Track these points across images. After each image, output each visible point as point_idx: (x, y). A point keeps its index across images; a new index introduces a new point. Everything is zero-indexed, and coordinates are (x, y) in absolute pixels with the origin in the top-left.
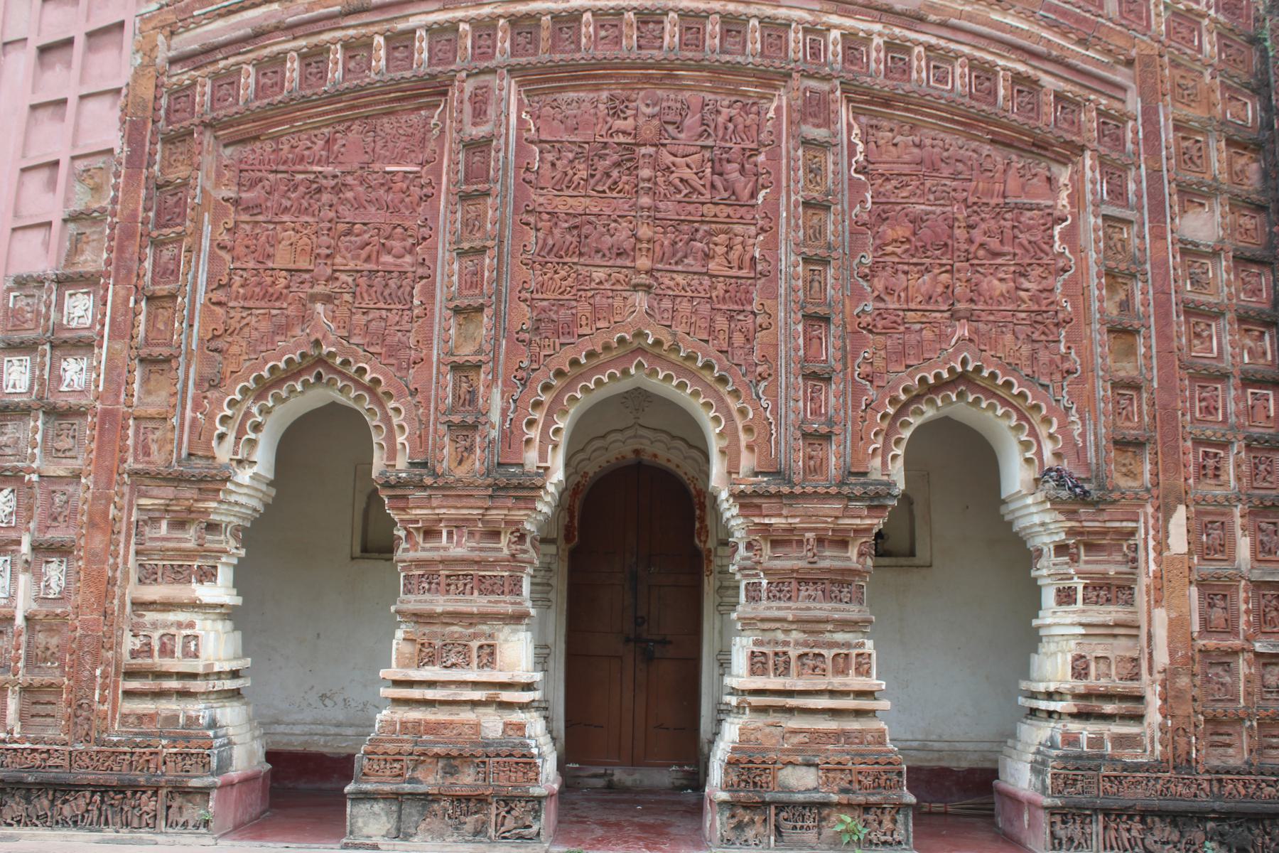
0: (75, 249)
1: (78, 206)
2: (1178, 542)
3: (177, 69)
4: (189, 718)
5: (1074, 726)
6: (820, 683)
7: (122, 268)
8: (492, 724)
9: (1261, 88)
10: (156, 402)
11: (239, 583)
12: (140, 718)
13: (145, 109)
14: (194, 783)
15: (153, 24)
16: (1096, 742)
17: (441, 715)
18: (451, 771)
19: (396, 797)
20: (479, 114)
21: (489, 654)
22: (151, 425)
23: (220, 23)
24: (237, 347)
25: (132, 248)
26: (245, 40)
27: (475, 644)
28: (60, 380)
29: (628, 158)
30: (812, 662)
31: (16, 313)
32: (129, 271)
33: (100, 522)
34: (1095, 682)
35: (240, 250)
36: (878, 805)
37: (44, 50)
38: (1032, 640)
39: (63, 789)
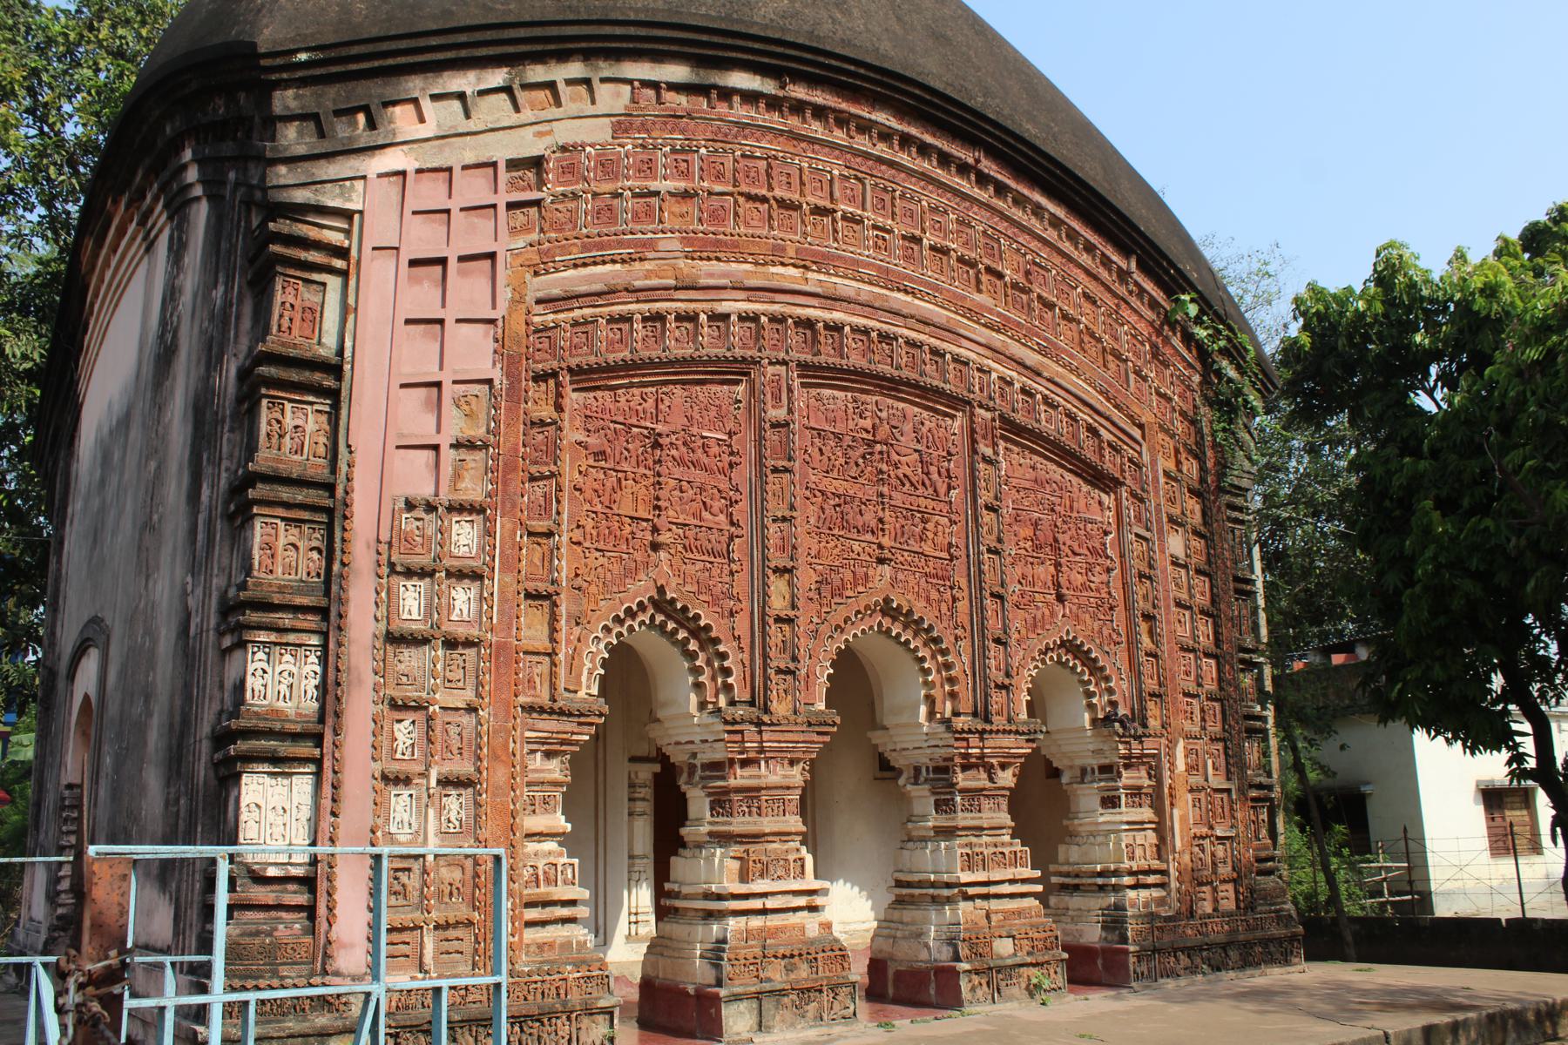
0: (457, 476)
3: (539, 309)
4: (578, 943)
5: (1132, 894)
6: (1009, 873)
9: (1199, 457)
12: (541, 947)
13: (519, 343)
14: (602, 1003)
15: (520, 261)
17: (774, 921)
18: (789, 969)
19: (758, 996)
22: (535, 658)
23: (571, 273)
26: (599, 294)
27: (791, 857)
28: (450, 608)
32: (514, 506)
35: (589, 494)
36: (1048, 962)
37: (414, 263)
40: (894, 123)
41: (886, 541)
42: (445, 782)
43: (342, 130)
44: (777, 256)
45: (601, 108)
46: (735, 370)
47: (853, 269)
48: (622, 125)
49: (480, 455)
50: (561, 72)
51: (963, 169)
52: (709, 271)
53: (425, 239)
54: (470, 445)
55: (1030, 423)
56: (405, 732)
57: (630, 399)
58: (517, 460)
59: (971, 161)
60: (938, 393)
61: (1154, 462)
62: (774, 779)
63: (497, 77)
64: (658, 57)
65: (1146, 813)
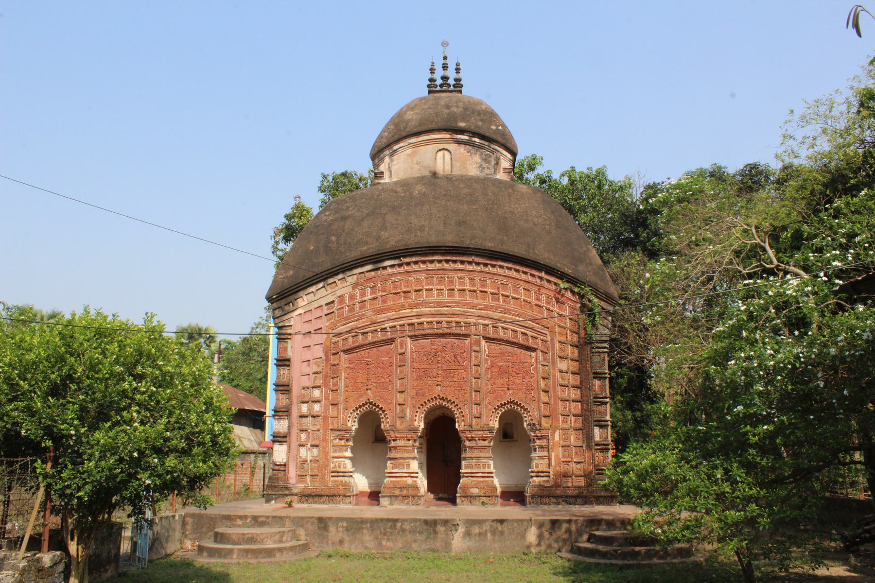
0: (315, 380)
2: (557, 438)
5: (535, 478)
7: (326, 384)
8: (410, 481)
10: (335, 413)
11: (352, 452)
16: (539, 482)
19: (390, 496)
20: (402, 346)
21: (408, 465)
25: (328, 380)
29: (435, 356)
30: (478, 466)
31: (304, 395)
33: (325, 440)
34: (540, 469)
38: (530, 460)
39: (320, 496)
40: (441, 258)
41: (439, 379)
42: (312, 446)
43: (287, 308)
44: (403, 307)
46: (392, 341)
47: (427, 304)
48: (355, 285)
49: (320, 375)
51: (470, 263)
54: (317, 373)
55: (496, 336)
56: (303, 436)
57: (361, 354)
58: (331, 373)
59: (471, 260)
60: (459, 335)
61: (552, 340)
63: (321, 285)
64: (362, 266)
65: (546, 453)
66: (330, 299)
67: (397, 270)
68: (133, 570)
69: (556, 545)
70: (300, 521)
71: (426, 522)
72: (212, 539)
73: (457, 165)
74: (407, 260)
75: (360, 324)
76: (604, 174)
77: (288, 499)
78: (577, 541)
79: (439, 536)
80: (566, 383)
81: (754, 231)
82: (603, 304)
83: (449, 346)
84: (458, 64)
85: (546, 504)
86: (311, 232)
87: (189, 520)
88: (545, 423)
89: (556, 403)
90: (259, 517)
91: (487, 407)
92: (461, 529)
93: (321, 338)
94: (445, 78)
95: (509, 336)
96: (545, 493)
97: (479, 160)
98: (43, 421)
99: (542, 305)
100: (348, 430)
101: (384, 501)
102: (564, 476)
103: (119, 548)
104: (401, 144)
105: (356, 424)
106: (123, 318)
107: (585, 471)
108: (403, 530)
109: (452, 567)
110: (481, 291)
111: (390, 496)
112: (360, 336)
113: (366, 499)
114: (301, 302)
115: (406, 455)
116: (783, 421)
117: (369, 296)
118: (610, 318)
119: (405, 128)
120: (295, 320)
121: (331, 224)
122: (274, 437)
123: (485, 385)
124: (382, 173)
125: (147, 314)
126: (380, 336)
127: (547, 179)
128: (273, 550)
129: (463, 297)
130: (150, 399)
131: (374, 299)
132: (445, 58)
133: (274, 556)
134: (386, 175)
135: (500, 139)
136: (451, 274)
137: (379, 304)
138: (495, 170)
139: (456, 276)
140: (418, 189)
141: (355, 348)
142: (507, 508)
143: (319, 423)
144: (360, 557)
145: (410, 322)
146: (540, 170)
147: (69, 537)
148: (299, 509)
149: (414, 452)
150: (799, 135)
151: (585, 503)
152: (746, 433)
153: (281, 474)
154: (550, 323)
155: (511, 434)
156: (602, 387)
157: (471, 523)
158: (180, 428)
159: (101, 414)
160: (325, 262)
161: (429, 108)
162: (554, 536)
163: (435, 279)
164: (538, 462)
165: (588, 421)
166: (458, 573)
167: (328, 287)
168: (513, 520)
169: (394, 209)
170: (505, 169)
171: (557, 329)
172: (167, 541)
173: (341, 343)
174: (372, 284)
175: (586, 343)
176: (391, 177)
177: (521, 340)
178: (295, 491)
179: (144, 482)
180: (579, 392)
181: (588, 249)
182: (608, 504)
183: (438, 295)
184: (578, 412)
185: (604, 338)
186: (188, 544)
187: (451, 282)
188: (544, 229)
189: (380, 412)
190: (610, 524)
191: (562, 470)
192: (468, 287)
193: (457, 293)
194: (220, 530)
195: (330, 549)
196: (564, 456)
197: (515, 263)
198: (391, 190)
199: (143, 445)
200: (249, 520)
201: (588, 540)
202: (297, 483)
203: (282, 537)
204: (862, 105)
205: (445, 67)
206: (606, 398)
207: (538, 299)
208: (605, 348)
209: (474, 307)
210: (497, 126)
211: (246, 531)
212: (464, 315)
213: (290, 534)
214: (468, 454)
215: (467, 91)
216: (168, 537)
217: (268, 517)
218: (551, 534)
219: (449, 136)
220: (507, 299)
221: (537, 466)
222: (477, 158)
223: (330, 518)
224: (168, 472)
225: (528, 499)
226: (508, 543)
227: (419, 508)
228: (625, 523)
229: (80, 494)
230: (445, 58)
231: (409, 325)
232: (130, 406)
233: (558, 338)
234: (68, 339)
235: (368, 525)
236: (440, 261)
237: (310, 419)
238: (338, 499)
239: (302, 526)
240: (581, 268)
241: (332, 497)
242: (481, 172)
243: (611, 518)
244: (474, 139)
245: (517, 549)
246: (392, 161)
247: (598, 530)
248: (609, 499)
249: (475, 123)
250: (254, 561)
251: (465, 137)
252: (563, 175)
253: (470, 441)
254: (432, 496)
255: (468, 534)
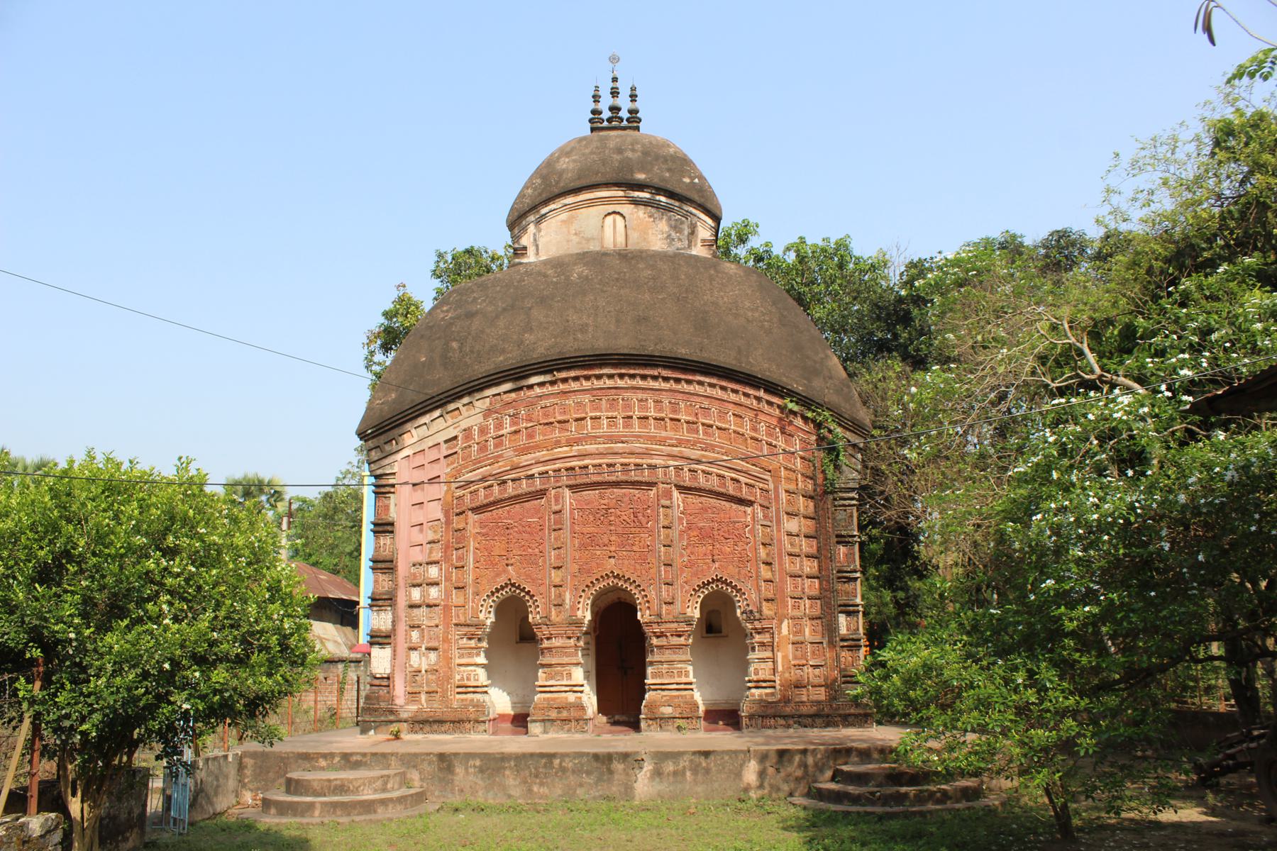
0: (431, 552)
1: (430, 538)
2: (785, 630)
5: (753, 691)
7: (447, 558)
8: (571, 697)
10: (461, 601)
11: (486, 657)
19: (543, 721)
20: (557, 501)
21: (569, 675)
24: (484, 582)
33: (446, 640)
34: (761, 677)
38: (747, 664)
39: (441, 722)
41: (613, 548)
42: (428, 649)
43: (387, 448)
44: (558, 444)
45: (478, 410)
46: (541, 493)
47: (593, 439)
48: (487, 413)
49: (439, 545)
50: (458, 404)
51: (655, 378)
52: (525, 459)
53: (418, 476)
55: (696, 485)
56: (415, 635)
58: (453, 542)
59: (656, 373)
61: (776, 489)
62: (558, 644)
63: (437, 413)
65: (769, 654)
66: (451, 433)
67: (548, 389)
68: (166, 837)
69: (786, 788)
70: (411, 760)
71: (596, 757)
72: (283, 789)
73: (634, 236)
74: (564, 375)
75: (495, 469)
76: (846, 247)
77: (394, 727)
78: (815, 781)
79: (616, 777)
80: (797, 550)
81: (1066, 326)
82: (848, 435)
83: (626, 499)
84: (633, 89)
85: (770, 727)
86: (422, 337)
87: (249, 762)
88: (767, 610)
89: (782, 580)
90: (352, 754)
91: (682, 587)
92: (648, 766)
93: (439, 491)
94: (615, 109)
95: (714, 483)
96: (770, 711)
97: (666, 229)
98: (27, 619)
99: (760, 437)
100: (479, 625)
101: (535, 728)
102: (796, 687)
103: (145, 805)
104: (552, 206)
105: (492, 615)
106: (144, 466)
107: (826, 678)
108: (563, 769)
109: (635, 822)
110: (672, 419)
111: (543, 721)
112: (496, 488)
113: (508, 725)
114: (407, 439)
115: (565, 660)
116: (1112, 600)
117: (507, 429)
118: (859, 456)
119: (557, 182)
120: (400, 466)
121: (451, 324)
122: (372, 637)
123: (679, 556)
124: (525, 248)
125: (180, 458)
126: (525, 486)
127: (765, 255)
128: (373, 802)
129: (646, 427)
130: (187, 584)
131: (516, 432)
132: (615, 80)
133: (375, 812)
134: (531, 251)
135: (696, 198)
136: (627, 395)
137: (522, 440)
138: (690, 242)
139: (634, 397)
140: (578, 271)
141: (491, 504)
142: (714, 734)
143: (437, 616)
144: (500, 810)
145: (569, 465)
146: (755, 242)
147: (69, 791)
148: (409, 742)
149: (576, 655)
150: (1128, 186)
151: (827, 725)
152: (1059, 618)
153: (383, 692)
154: (773, 464)
155: (719, 626)
156: (850, 556)
157: (662, 756)
158: (232, 626)
159: (114, 608)
160: (443, 380)
161: (592, 153)
162: (782, 774)
163: (604, 402)
164: (758, 667)
165: (830, 605)
166: (644, 830)
167: (447, 417)
168: (723, 752)
169: (543, 301)
170: (704, 241)
171: (783, 472)
172: (216, 794)
173: (468, 498)
174: (511, 411)
175: (825, 493)
176: (537, 253)
177: (731, 489)
178: (404, 715)
179: (180, 707)
180: (816, 564)
181: (827, 356)
182: (861, 726)
183: (609, 426)
184: (815, 592)
185: (852, 485)
186: (248, 797)
187: (628, 406)
188: (762, 327)
189: (527, 598)
190: (865, 755)
191: (794, 679)
192: (652, 413)
193: (636, 422)
194: (294, 775)
195: (456, 800)
196: (795, 658)
197: (720, 377)
198: (538, 272)
199: (178, 652)
200: (337, 759)
201: (833, 779)
202: (407, 704)
203: (386, 783)
204: (1217, 143)
205: (615, 93)
206: (855, 571)
207: (755, 429)
208: (853, 499)
209: (662, 442)
210: (692, 179)
211: (332, 775)
212: (647, 454)
213: (398, 779)
214: (656, 658)
215: (647, 127)
216: (218, 786)
217: (364, 755)
218: (778, 770)
219: (621, 194)
220: (710, 430)
221: (756, 673)
222: (663, 225)
223: (456, 754)
224: (215, 692)
225: (745, 721)
226: (716, 785)
227: (587, 736)
228: (885, 752)
229: (84, 727)
230: (615, 80)
231: (567, 469)
232: (157, 595)
233: (784, 485)
234: (64, 498)
235: (512, 763)
236: (611, 376)
237: (424, 609)
238: (467, 725)
239: (415, 767)
240: (817, 383)
241: (457, 723)
242: (670, 244)
243: (864, 745)
244: (658, 198)
245: (730, 793)
246: (540, 231)
247: (846, 763)
248: (863, 719)
249: (659, 174)
250: (344, 820)
251: (645, 195)
252: (788, 249)
253: (658, 637)
254: (604, 719)
255: (657, 773)
